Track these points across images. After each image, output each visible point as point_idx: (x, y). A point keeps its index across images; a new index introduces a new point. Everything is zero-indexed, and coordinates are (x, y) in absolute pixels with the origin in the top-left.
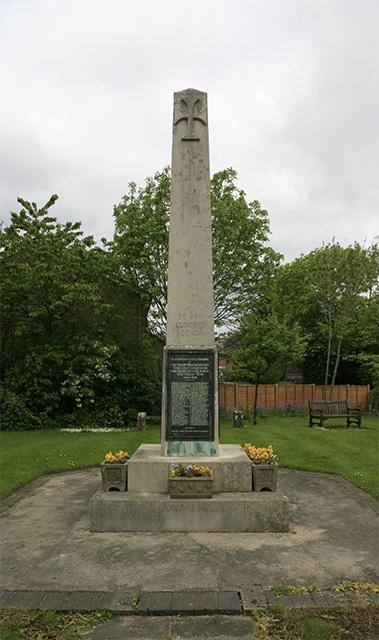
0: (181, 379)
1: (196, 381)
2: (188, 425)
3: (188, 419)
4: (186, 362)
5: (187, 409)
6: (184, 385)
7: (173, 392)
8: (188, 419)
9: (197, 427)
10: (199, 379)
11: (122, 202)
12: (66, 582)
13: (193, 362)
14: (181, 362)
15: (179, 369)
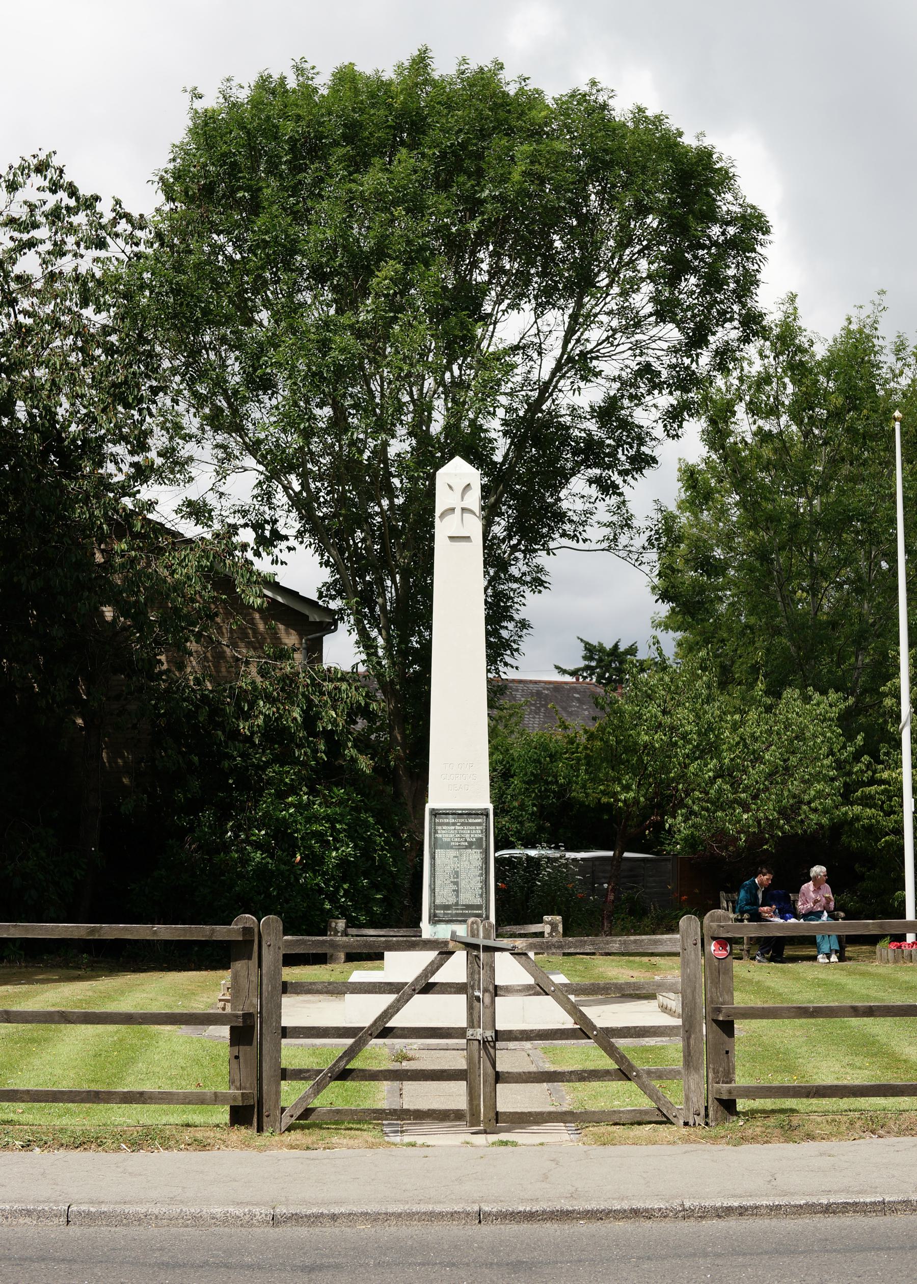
0: (447, 846)
1: (467, 848)
2: (457, 904)
3: (457, 896)
4: (454, 824)
5: (456, 883)
6: (452, 853)
7: (438, 861)
8: (457, 896)
9: (468, 907)
10: (470, 846)
11: (584, 89)
12: (566, 1227)
13: (463, 824)
14: (448, 824)
15: (446, 833)
